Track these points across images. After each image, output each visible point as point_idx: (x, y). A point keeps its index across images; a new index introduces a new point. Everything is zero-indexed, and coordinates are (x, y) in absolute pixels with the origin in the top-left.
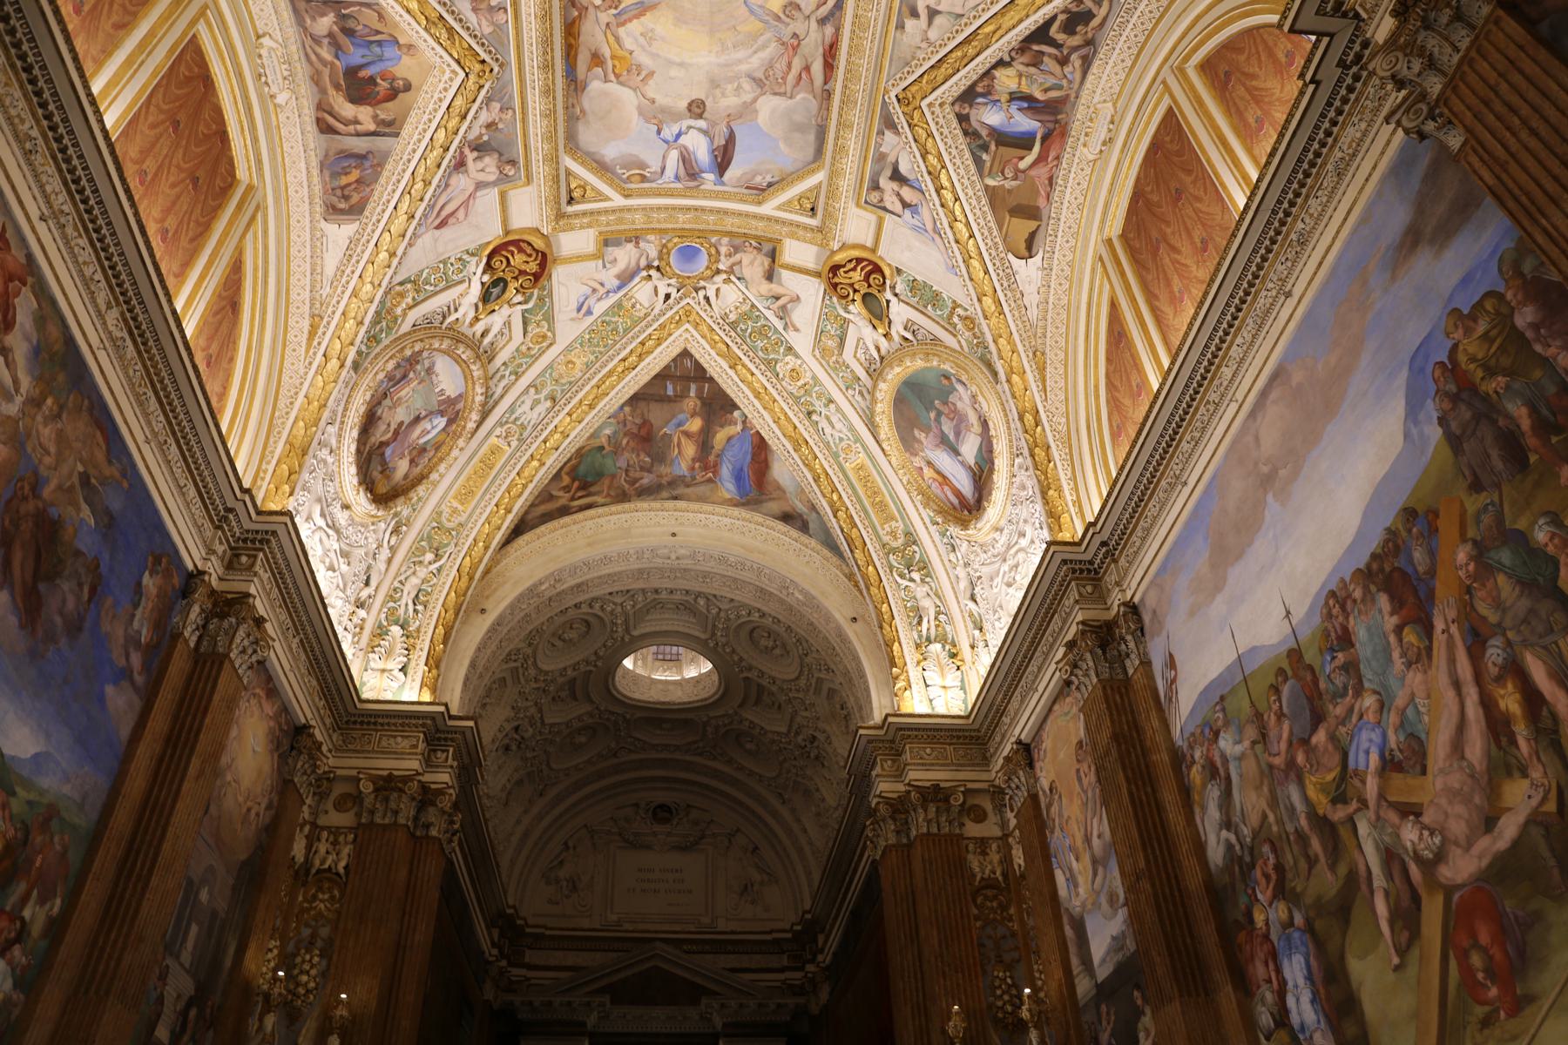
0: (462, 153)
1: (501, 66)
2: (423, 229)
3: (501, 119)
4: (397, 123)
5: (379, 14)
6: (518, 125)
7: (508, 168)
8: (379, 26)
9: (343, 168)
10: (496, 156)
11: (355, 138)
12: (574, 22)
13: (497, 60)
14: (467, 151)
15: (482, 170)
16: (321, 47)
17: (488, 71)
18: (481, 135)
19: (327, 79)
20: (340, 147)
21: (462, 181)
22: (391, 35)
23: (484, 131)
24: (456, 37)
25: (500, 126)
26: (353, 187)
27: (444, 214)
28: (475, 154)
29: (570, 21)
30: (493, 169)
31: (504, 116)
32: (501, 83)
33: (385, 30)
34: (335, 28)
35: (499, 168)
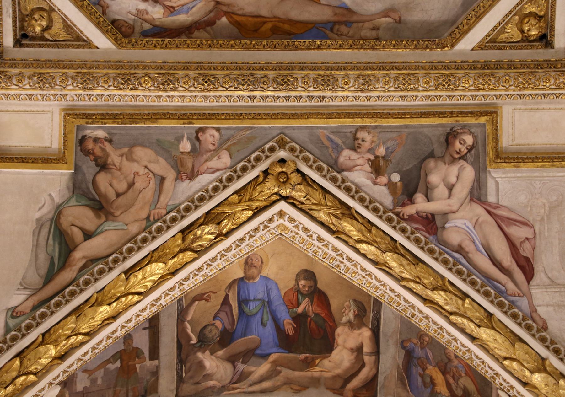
0: (411, 219)
1: (282, 145)
2: (523, 303)
3: (370, 151)
4: (360, 298)
5: (195, 299)
6: (383, 122)
7: (458, 145)
8: (216, 302)
9: (424, 383)
10: (431, 163)
11: (382, 357)
12: (237, 24)
13: (272, 150)
14: (410, 210)
15: (451, 188)
16: (250, 373)
17: (278, 169)
18: (390, 185)
19: (297, 374)
20: (394, 381)
21: (459, 223)
22: (230, 286)
23: (384, 179)
24: (221, 210)
25: (381, 151)
26: (451, 381)
27: (507, 260)
28: (419, 197)
29: (236, 30)
30: (454, 170)
31: (367, 145)
32: (310, 146)
33: (222, 295)
34: (220, 353)
35: (454, 160)
